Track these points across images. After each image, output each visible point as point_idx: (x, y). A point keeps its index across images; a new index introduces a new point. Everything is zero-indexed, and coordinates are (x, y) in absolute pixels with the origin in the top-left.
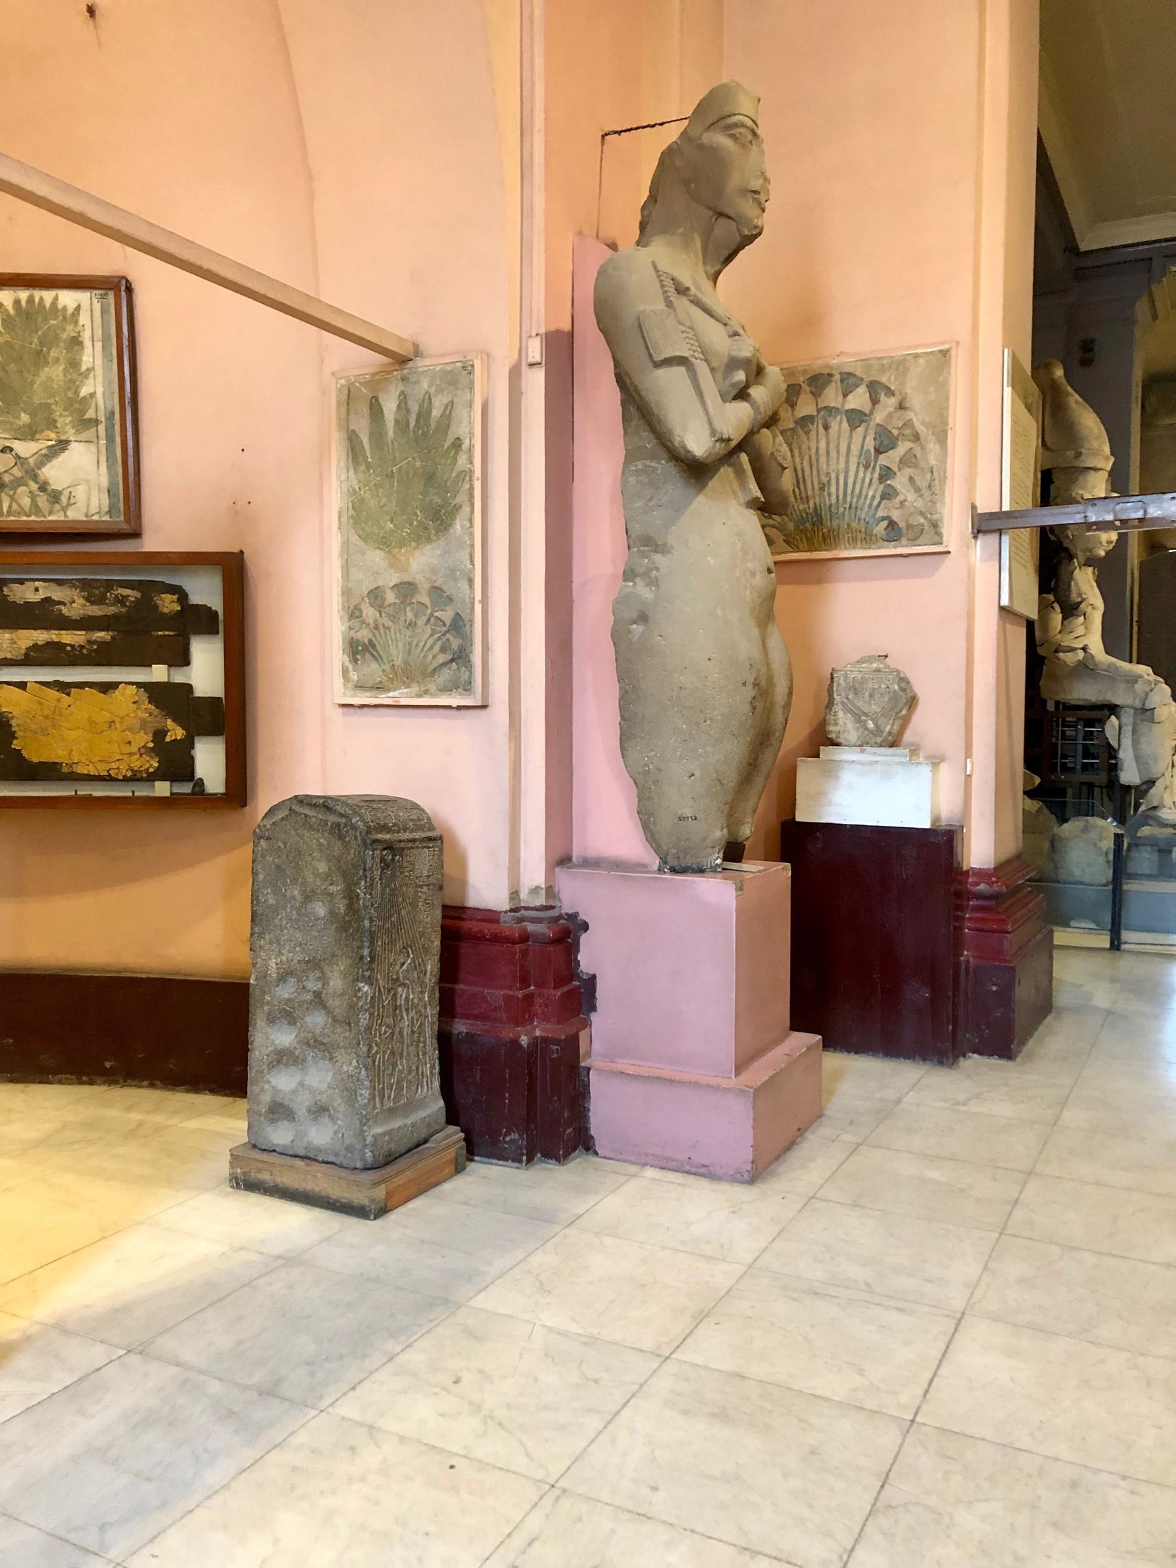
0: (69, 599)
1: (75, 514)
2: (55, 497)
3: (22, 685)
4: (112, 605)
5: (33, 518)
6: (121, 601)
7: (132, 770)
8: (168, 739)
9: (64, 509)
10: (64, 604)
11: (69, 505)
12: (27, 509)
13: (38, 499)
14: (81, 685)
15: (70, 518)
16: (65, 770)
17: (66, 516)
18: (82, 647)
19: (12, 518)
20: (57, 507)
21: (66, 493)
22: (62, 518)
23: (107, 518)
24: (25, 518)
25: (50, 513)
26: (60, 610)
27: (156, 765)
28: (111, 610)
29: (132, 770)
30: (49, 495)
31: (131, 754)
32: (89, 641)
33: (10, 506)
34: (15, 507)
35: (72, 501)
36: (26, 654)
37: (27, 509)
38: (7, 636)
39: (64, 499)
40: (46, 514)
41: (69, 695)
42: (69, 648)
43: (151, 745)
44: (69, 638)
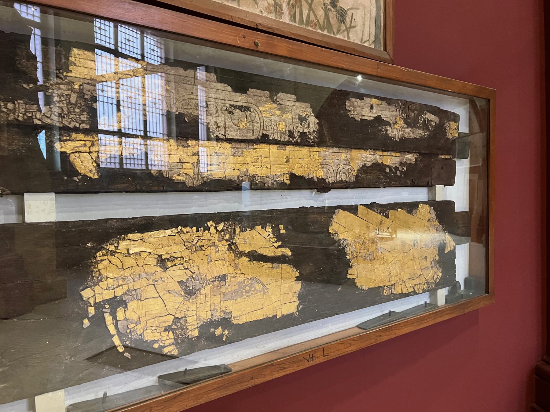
0: (393, 119)
1: (355, 38)
2: (342, 15)
3: (353, 209)
4: (420, 129)
5: (325, 33)
6: (426, 124)
7: (428, 283)
8: (446, 252)
9: (348, 30)
10: (388, 123)
11: (351, 27)
12: (321, 21)
13: (330, 14)
14: (395, 206)
15: (351, 41)
16: (386, 292)
17: (348, 37)
18: (396, 168)
19: (309, 28)
20: (343, 27)
21: (349, 13)
22: (346, 39)
23: (373, 46)
24: (320, 31)
25: (338, 31)
26: (387, 131)
27: (440, 275)
28: (419, 133)
29: (428, 283)
30: (337, 11)
31: (427, 268)
32: (401, 163)
33: (309, 15)
34: (312, 17)
35: (353, 24)
36: (357, 176)
37: (321, 21)
38: (344, 156)
39: (348, 20)
40: (335, 30)
41: (387, 216)
42: (388, 170)
43: (437, 258)
44: (391, 159)
